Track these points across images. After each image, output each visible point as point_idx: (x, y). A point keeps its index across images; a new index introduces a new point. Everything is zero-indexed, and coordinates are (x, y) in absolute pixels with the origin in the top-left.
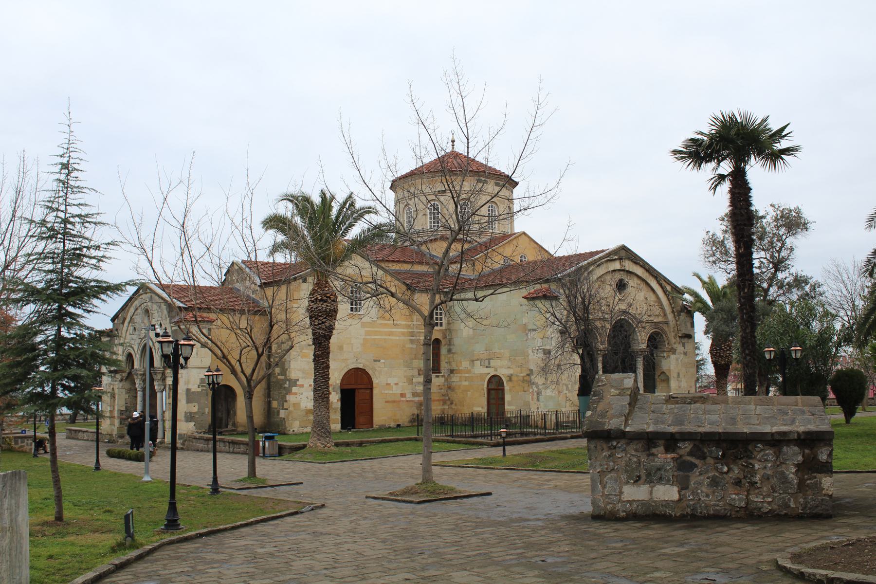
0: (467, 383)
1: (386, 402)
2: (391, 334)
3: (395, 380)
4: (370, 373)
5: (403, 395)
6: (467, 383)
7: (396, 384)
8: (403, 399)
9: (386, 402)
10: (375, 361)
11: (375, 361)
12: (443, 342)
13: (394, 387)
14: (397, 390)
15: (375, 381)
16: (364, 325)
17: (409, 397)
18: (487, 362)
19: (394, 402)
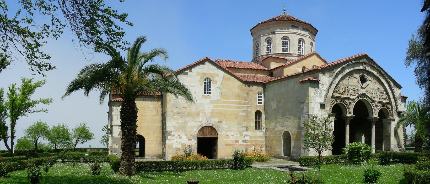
0: (273, 136)
1: (226, 145)
2: (229, 107)
3: (232, 133)
4: (216, 129)
5: (237, 141)
6: (273, 136)
7: (232, 135)
8: (237, 144)
9: (226, 145)
10: (219, 122)
11: (219, 122)
12: (263, 113)
13: (231, 137)
14: (232, 139)
15: (219, 133)
16: (211, 102)
17: (241, 142)
18: (283, 124)
19: (231, 145)
